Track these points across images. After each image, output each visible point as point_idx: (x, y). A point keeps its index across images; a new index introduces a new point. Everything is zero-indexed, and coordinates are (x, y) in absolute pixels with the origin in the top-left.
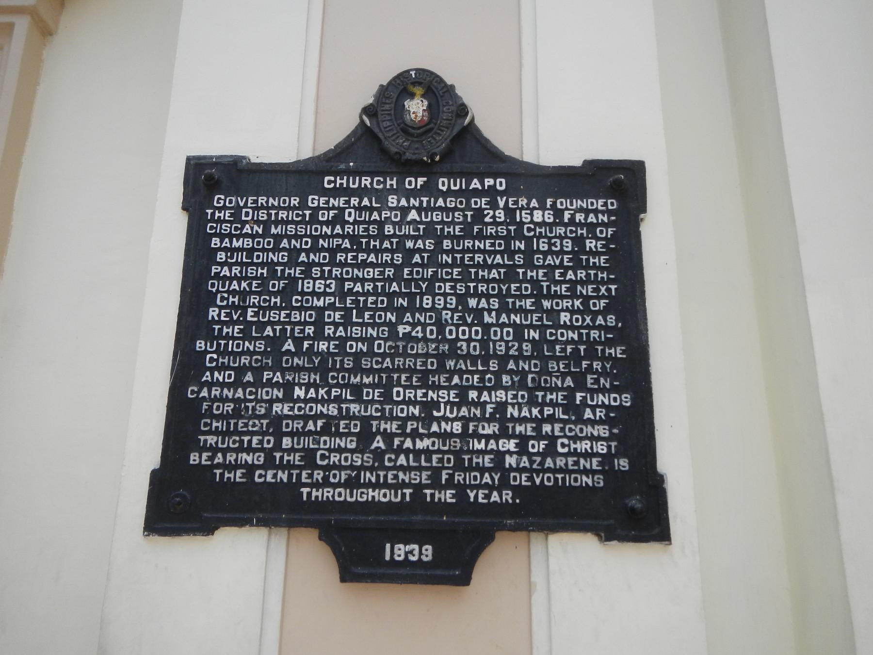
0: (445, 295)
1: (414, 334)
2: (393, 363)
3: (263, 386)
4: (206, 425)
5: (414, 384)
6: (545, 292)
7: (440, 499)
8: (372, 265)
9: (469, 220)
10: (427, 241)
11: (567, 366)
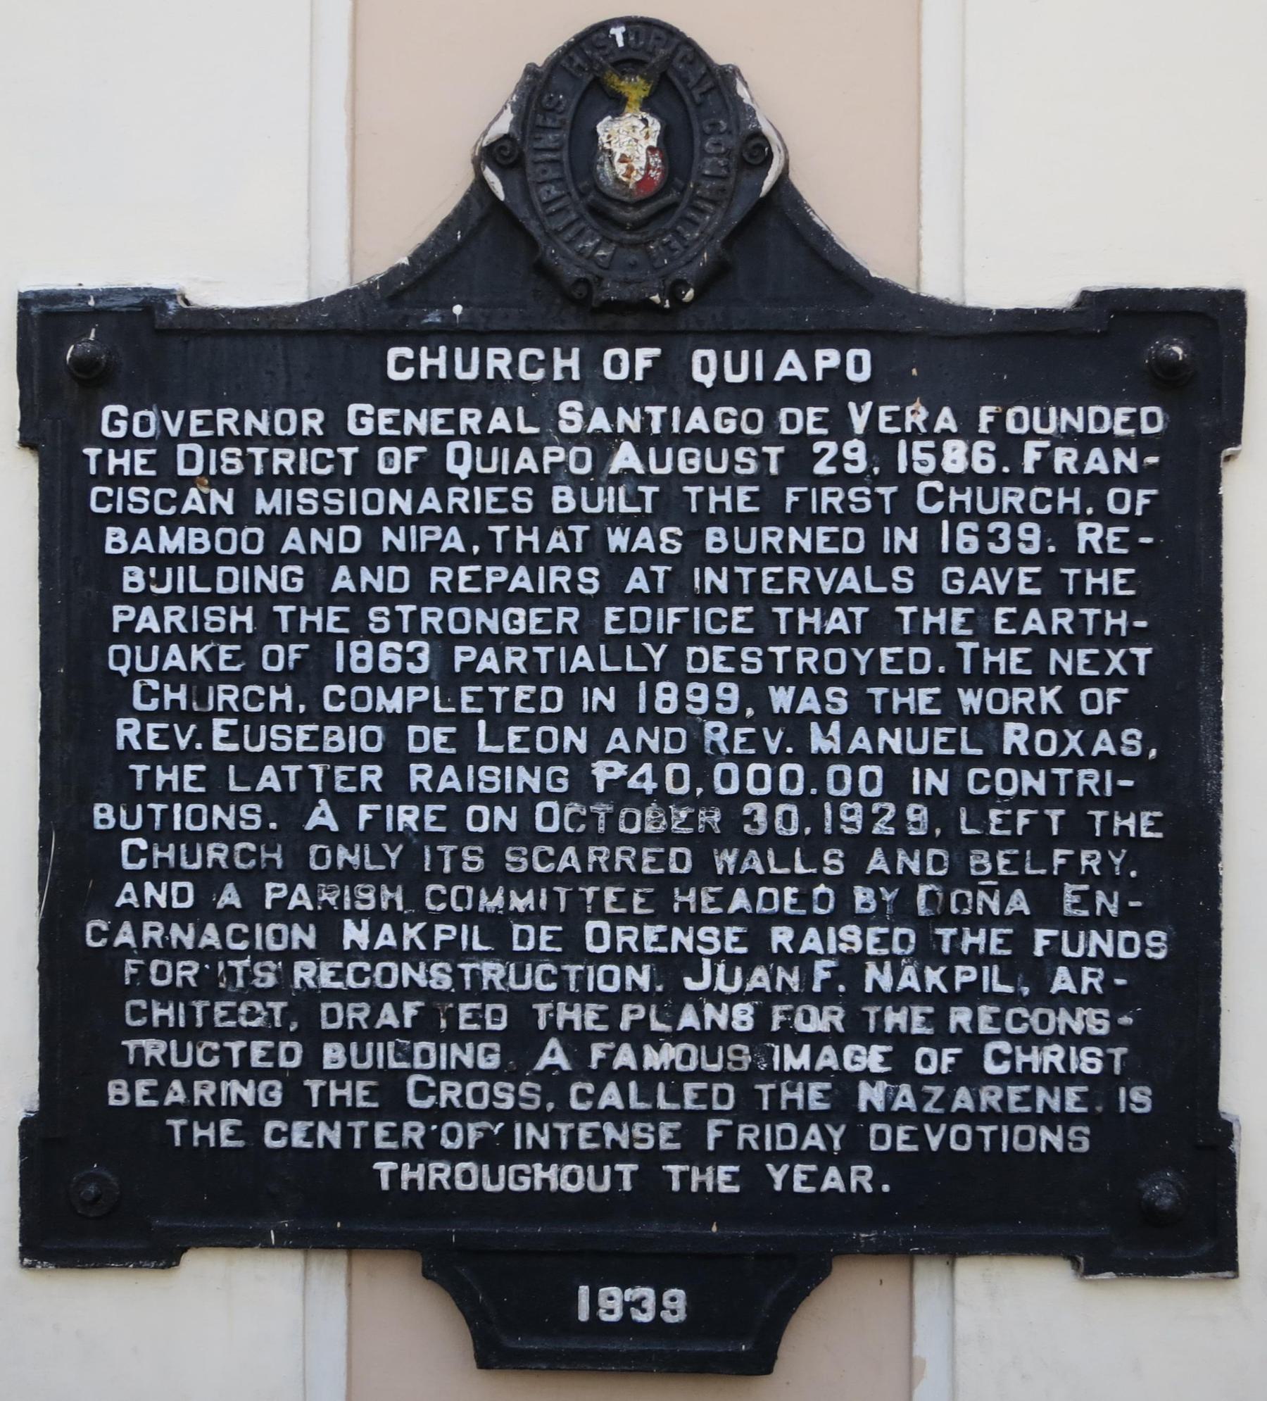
0: (711, 679)
1: (633, 783)
2: (583, 860)
3: (266, 918)
4: (136, 1012)
5: (637, 911)
6: (967, 669)
7: (702, 1185)
8: (522, 599)
9: (774, 469)
10: (664, 532)
11: (1016, 862)
